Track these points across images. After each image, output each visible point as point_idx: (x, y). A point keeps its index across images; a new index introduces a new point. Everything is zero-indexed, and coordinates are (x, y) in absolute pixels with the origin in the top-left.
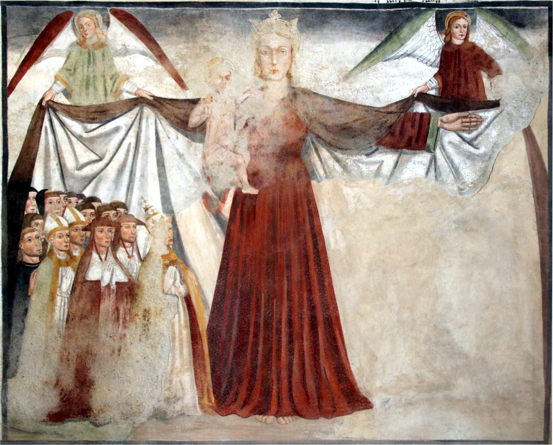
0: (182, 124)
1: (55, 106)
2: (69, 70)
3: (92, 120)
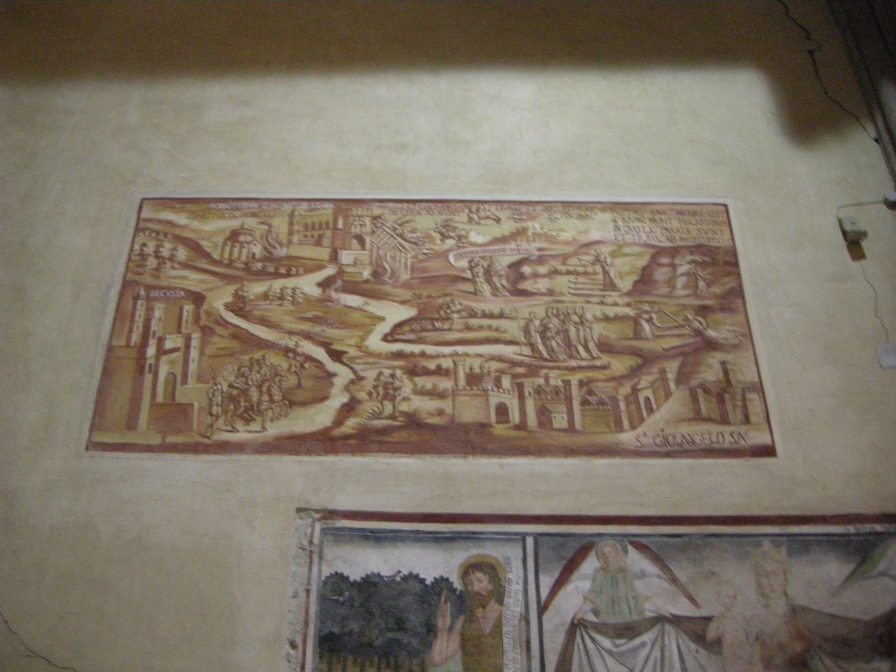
0: (699, 638)
1: (586, 623)
2: (596, 591)
3: (620, 636)
